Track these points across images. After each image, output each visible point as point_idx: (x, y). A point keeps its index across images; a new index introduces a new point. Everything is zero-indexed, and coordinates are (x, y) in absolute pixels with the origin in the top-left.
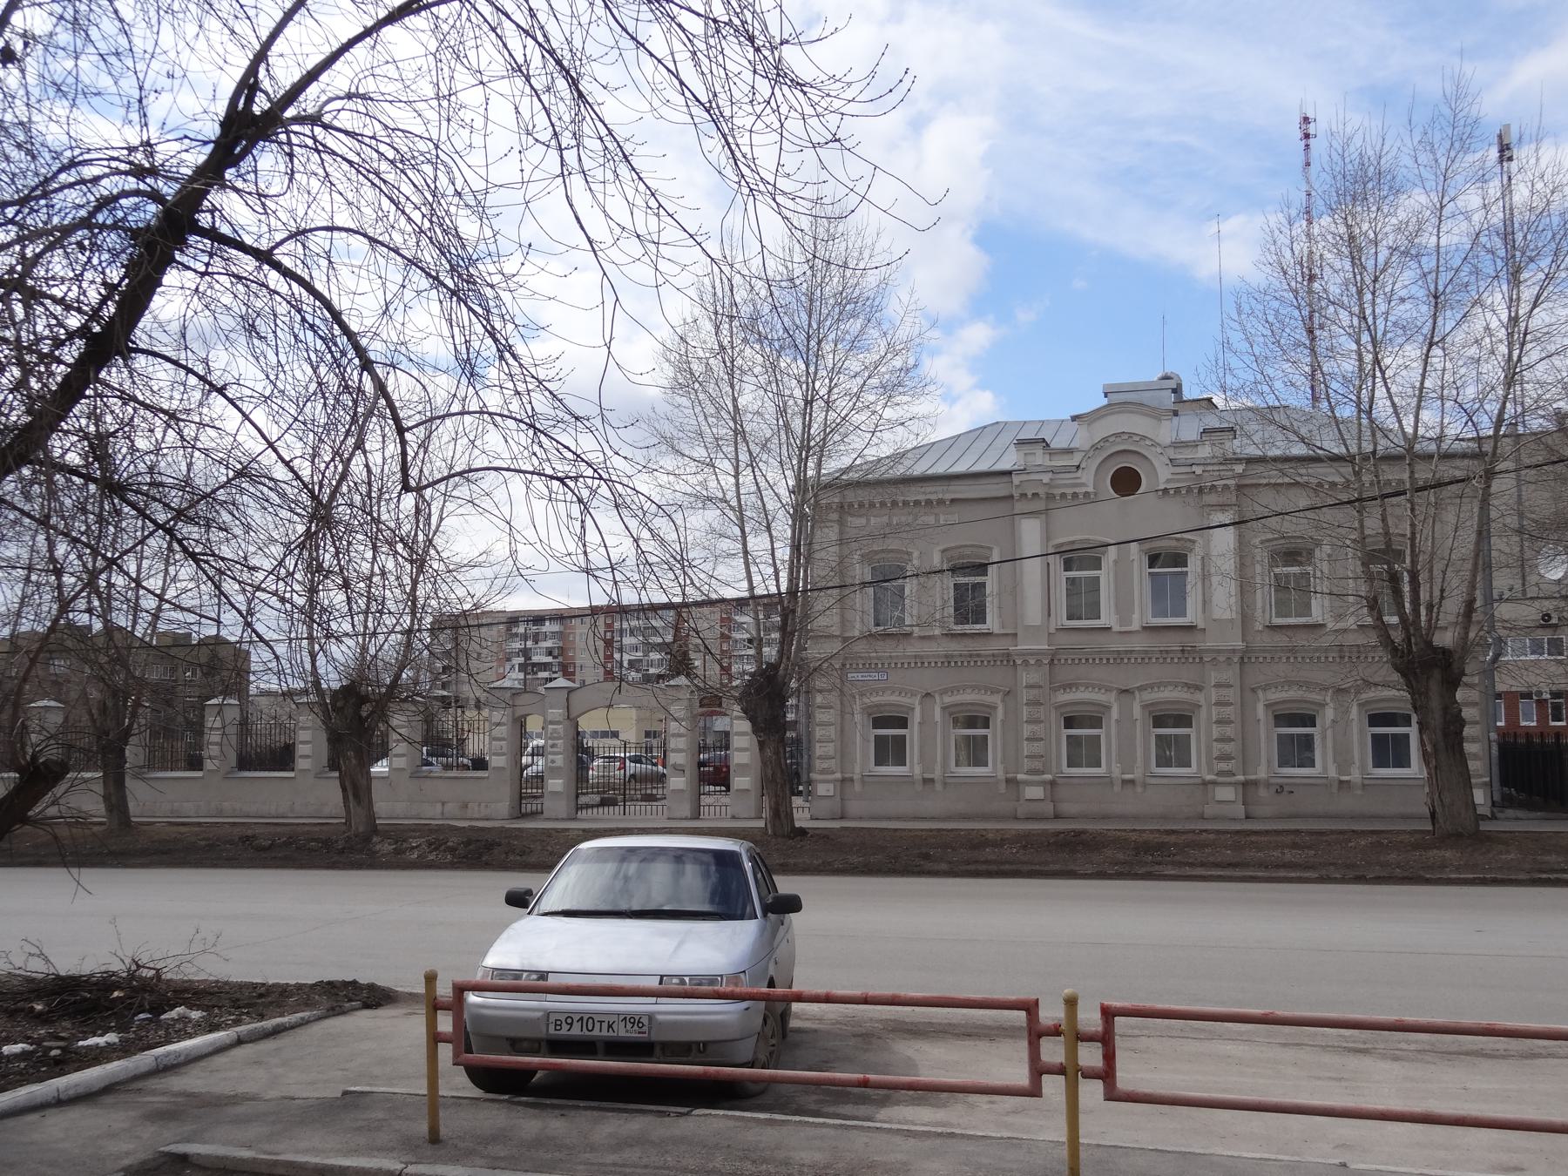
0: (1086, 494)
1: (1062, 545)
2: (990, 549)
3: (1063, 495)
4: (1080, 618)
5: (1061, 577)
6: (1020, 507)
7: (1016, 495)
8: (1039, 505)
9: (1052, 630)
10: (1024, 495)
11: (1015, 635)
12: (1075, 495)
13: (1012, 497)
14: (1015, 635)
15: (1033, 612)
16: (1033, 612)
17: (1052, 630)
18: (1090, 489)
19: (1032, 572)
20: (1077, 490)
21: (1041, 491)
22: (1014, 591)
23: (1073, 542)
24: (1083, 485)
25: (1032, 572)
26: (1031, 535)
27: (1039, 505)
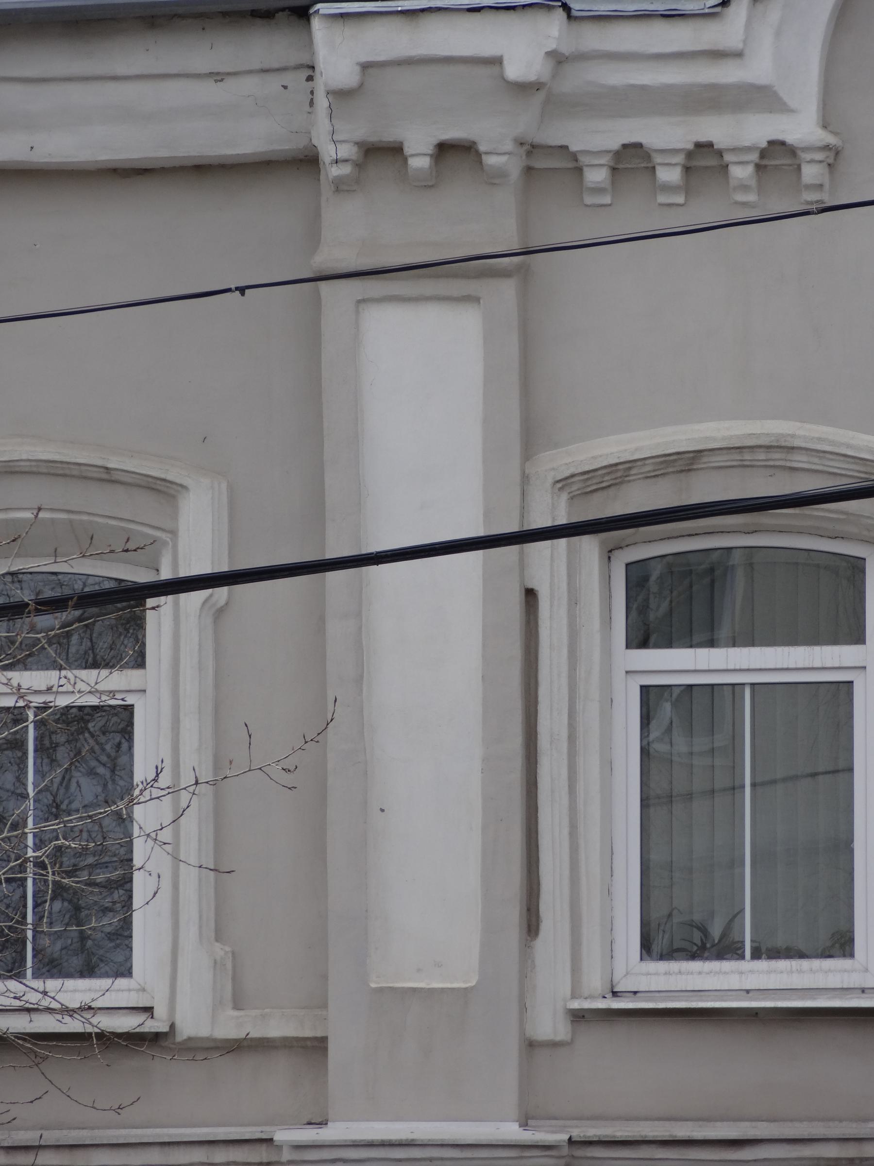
0: (776, 157)
1: (618, 474)
2: (164, 491)
3: (631, 160)
4: (727, 949)
5: (609, 677)
6: (353, 228)
7: (335, 150)
8: (479, 220)
9: (549, 1025)
10: (381, 154)
11: (317, 1047)
12: (704, 162)
13: (308, 162)
14: (317, 1047)
15: (428, 908)
16: (428, 908)
17: (549, 1025)
18: (802, 128)
19: (428, 639)
20: (717, 130)
21: (496, 134)
22: (306, 763)
23: (686, 462)
24: (760, 98)
25: (428, 639)
26: (421, 409)
27: (479, 220)
